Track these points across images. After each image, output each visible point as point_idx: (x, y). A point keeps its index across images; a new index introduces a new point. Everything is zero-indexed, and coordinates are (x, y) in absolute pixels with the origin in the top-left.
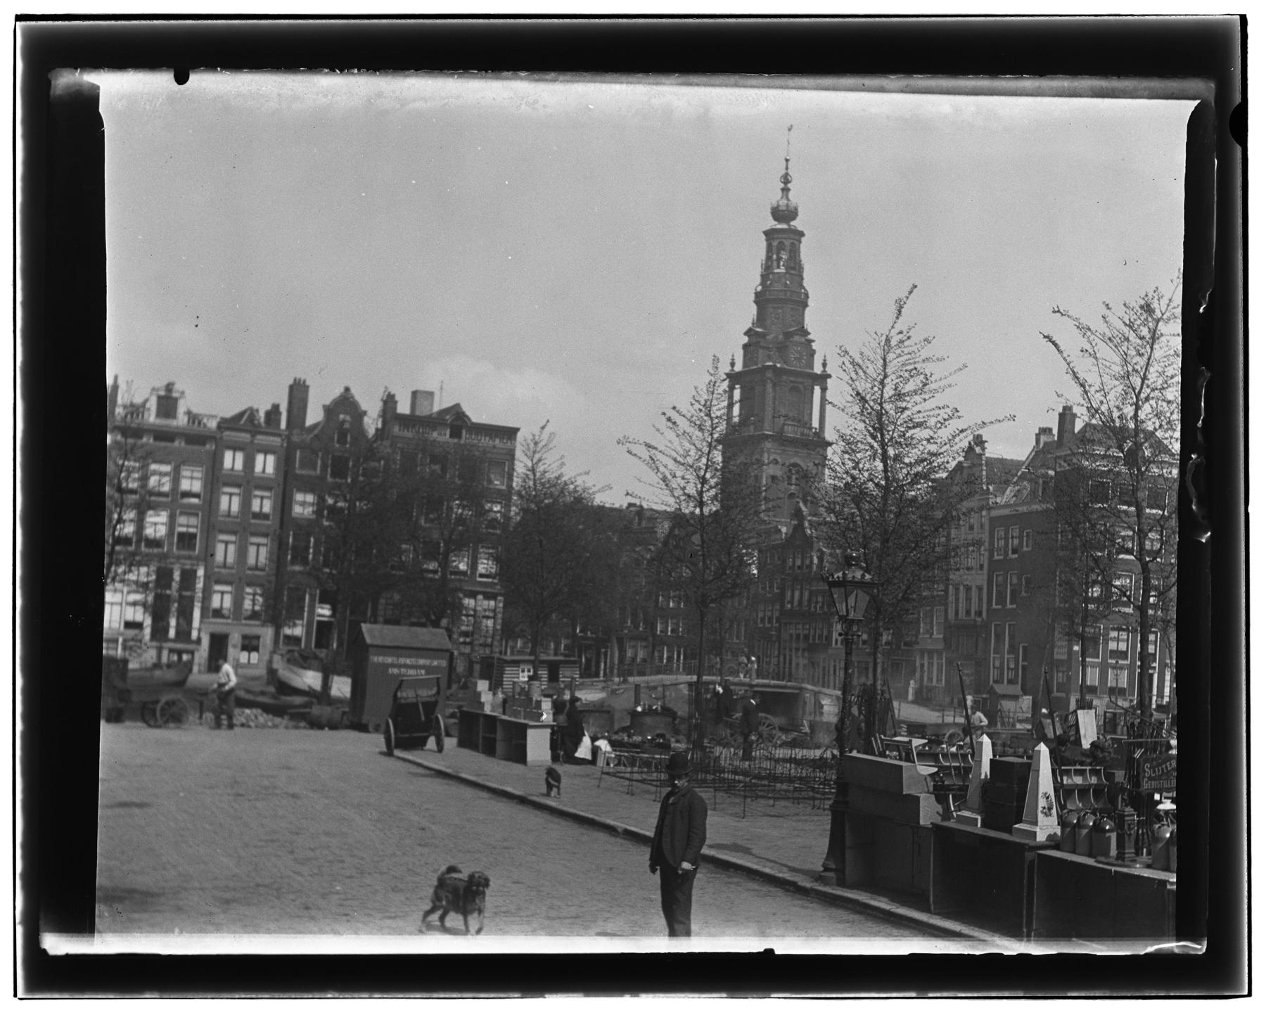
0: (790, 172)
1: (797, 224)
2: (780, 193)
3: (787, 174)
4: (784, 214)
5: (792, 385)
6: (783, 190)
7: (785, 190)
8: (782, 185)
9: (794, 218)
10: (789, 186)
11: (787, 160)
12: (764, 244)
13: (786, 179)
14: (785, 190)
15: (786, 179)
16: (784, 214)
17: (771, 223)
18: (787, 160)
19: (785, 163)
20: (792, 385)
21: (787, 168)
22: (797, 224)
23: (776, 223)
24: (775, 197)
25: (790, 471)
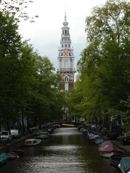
0: (66, 15)
1: (68, 26)
2: (64, 20)
4: (66, 24)
5: (65, 60)
6: (65, 19)
7: (65, 19)
8: (65, 18)
9: (67, 25)
10: (66, 18)
11: (65, 13)
12: (62, 31)
13: (65, 17)
14: (65, 19)
15: (65, 17)
16: (66, 24)
17: (63, 26)
18: (65, 13)
20: (65, 60)
22: (68, 26)
23: (64, 26)
24: (64, 21)
25: (65, 78)
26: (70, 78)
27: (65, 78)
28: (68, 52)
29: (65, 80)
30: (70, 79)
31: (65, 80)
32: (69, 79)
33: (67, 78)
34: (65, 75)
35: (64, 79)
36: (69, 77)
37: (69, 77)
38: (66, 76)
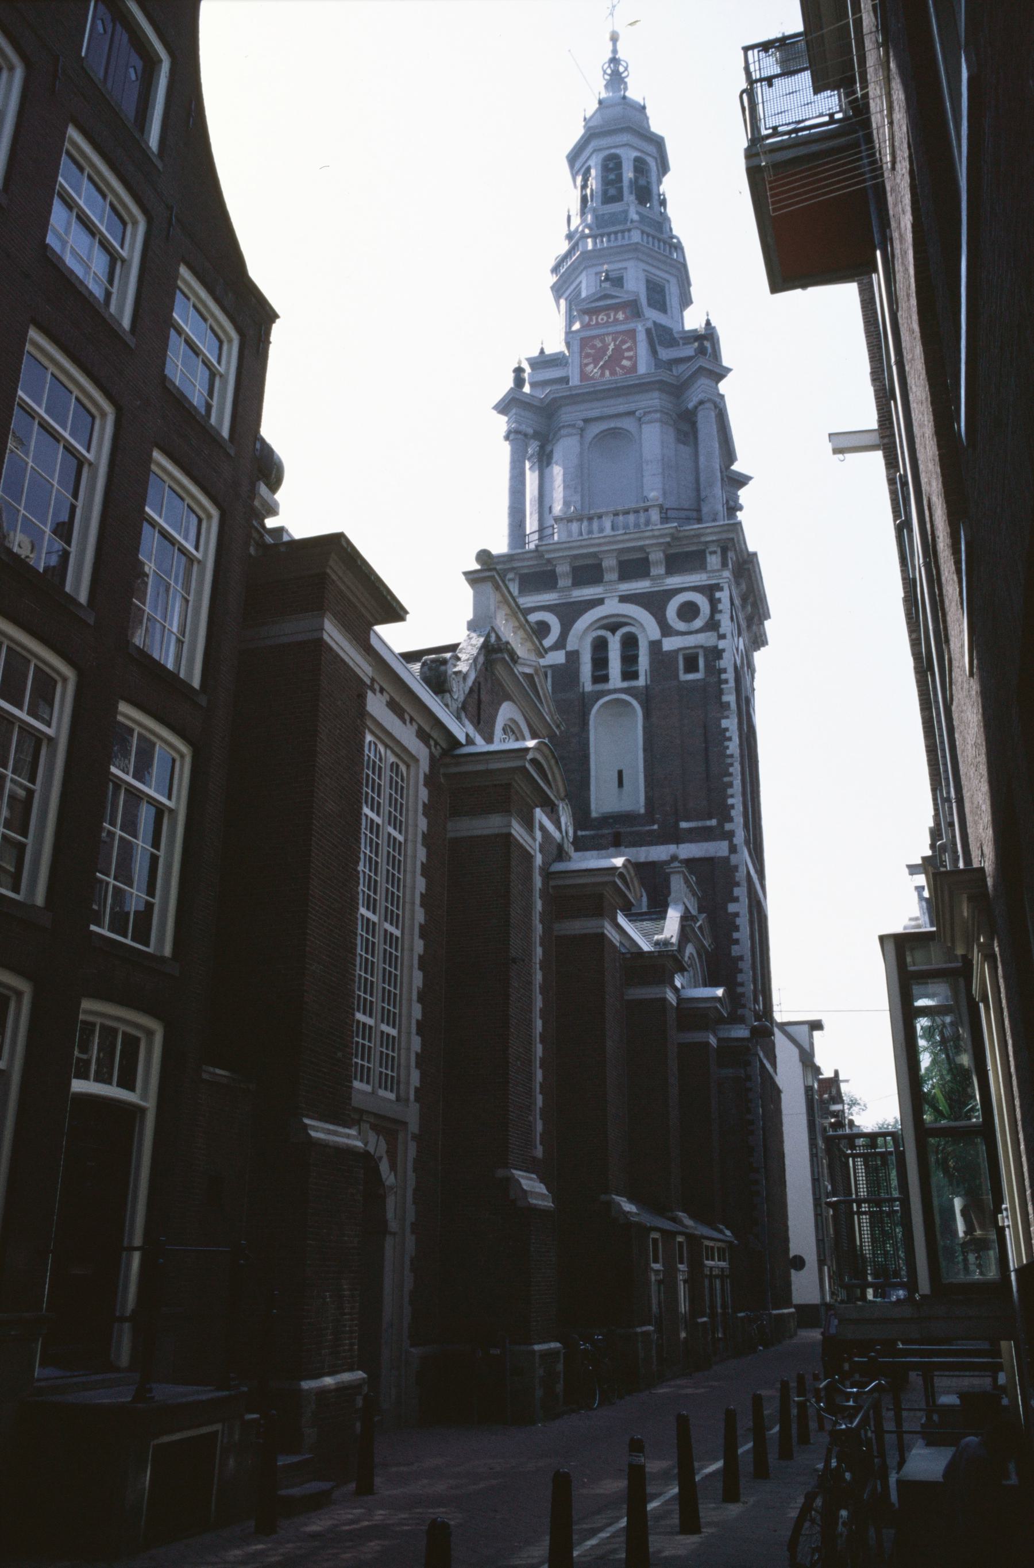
3: (614, 61)
11: (614, 38)
18: (614, 38)
19: (610, 44)
21: (615, 51)
25: (600, 647)
26: (667, 630)
27: (600, 647)
28: (632, 334)
29: (600, 662)
30: (670, 644)
31: (600, 662)
32: (655, 646)
33: (630, 643)
34: (600, 602)
35: (573, 657)
36: (648, 627)
37: (648, 627)
38: (612, 607)
